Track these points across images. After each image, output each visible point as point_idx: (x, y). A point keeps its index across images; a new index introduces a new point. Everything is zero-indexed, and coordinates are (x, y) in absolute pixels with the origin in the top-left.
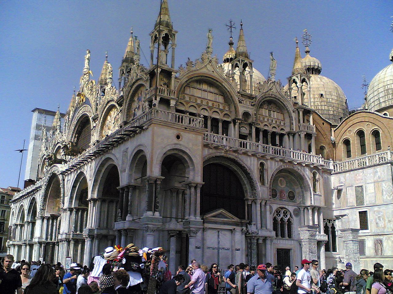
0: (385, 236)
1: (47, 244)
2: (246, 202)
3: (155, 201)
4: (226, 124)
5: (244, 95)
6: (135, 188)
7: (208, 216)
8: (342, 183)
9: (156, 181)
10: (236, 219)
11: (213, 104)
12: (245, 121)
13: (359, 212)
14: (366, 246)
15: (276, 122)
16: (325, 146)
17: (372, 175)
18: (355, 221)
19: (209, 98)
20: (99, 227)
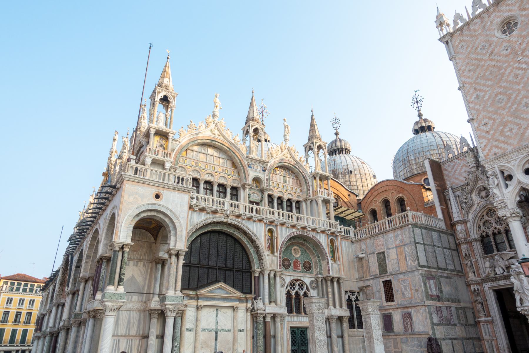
8: (363, 250)
9: (122, 248)
10: (239, 294)
13: (383, 282)
14: (394, 321)
17: (393, 239)
18: (380, 292)
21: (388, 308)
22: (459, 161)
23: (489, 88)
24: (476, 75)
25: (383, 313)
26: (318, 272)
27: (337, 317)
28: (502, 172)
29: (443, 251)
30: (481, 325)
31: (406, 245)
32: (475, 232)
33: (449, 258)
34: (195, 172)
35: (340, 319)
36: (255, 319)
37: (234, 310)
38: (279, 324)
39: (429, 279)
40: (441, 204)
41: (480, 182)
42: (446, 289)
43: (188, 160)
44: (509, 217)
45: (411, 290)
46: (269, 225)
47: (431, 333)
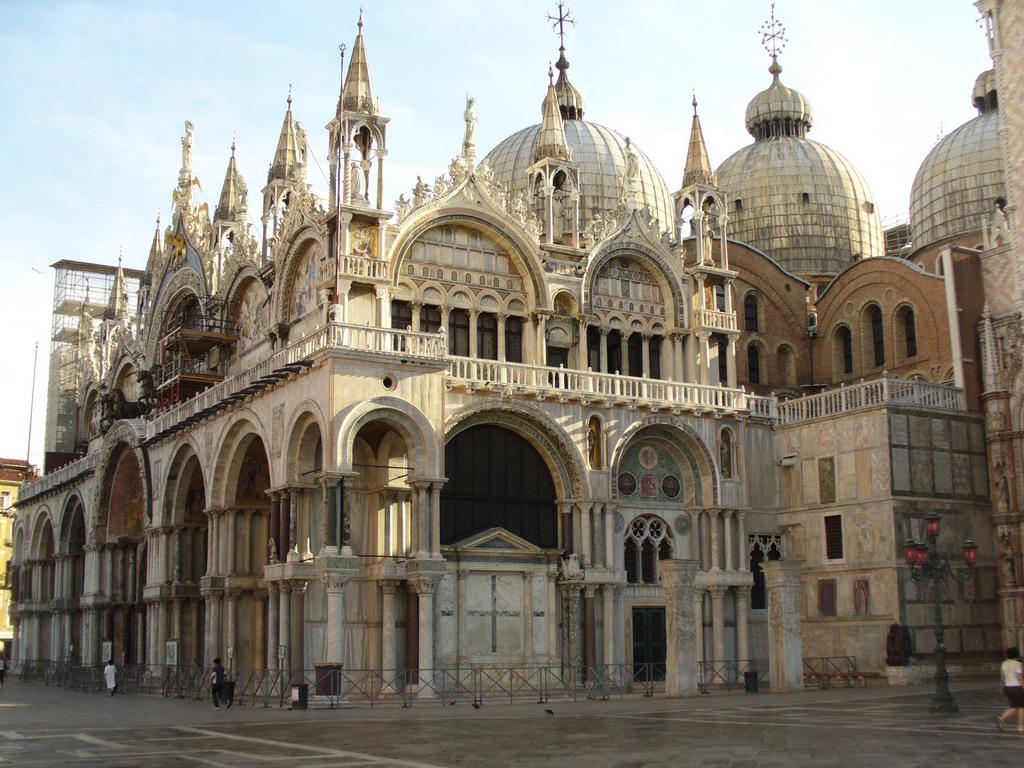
0: (874, 573)
1: (115, 608)
2: (559, 509)
3: (342, 522)
4: (515, 325)
6: (302, 492)
7: (469, 545)
8: (793, 450)
9: (341, 482)
10: (534, 549)
11: (482, 279)
12: (564, 312)
13: (826, 518)
15: (642, 307)
16: (790, 343)
17: (851, 433)
18: (818, 538)
19: (472, 265)
20: (235, 572)
21: (829, 569)
25: (820, 578)
26: (692, 501)
27: (726, 588)
29: (952, 458)
30: (1005, 602)
31: (873, 448)
33: (963, 471)
34: (430, 292)
35: (732, 591)
36: (564, 593)
37: (525, 577)
38: (611, 603)
39: (907, 516)
40: (964, 353)
45: (873, 539)
46: (592, 409)
47: (897, 619)
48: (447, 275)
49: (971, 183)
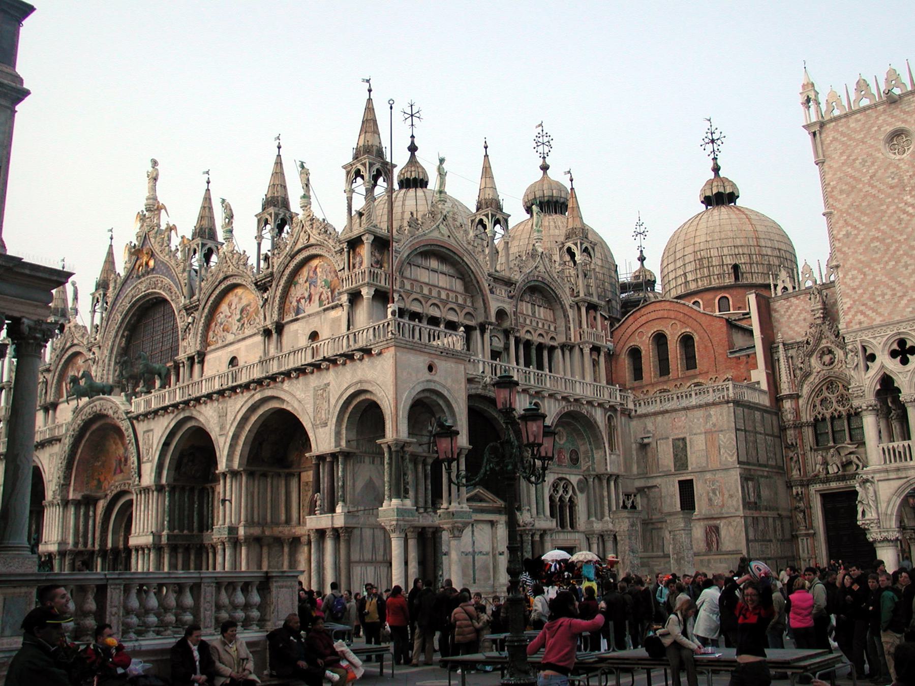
1: (81, 553)
5: (497, 280)
8: (649, 432)
10: (500, 503)
11: (448, 295)
13: (679, 482)
15: (543, 325)
17: (701, 420)
18: (673, 496)
19: (441, 284)
22: (797, 302)
23: (864, 227)
24: (850, 200)
28: (864, 349)
31: (722, 431)
32: (808, 412)
41: (824, 341)
42: (765, 493)
43: (405, 281)
44: (865, 410)
47: (745, 552)
48: (426, 291)
49: (714, 253)
